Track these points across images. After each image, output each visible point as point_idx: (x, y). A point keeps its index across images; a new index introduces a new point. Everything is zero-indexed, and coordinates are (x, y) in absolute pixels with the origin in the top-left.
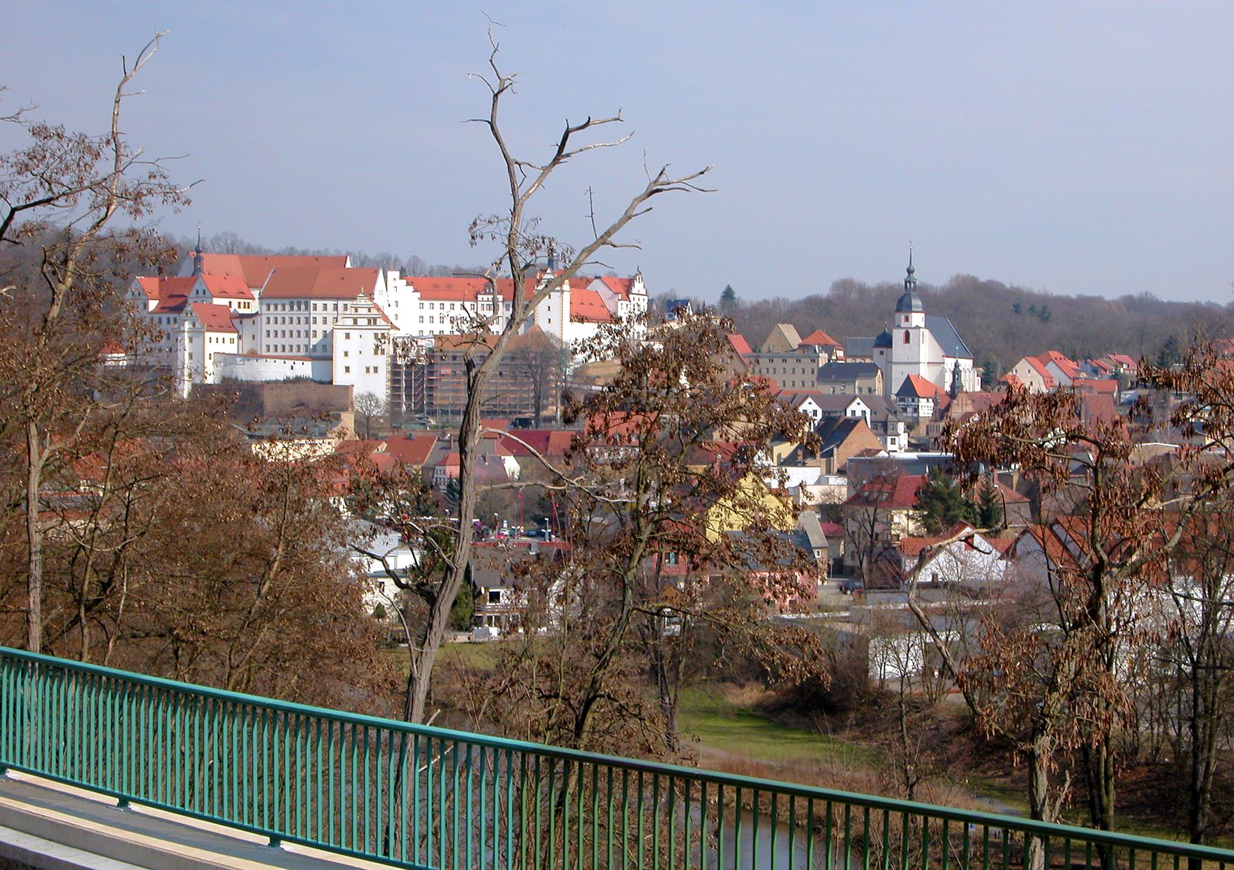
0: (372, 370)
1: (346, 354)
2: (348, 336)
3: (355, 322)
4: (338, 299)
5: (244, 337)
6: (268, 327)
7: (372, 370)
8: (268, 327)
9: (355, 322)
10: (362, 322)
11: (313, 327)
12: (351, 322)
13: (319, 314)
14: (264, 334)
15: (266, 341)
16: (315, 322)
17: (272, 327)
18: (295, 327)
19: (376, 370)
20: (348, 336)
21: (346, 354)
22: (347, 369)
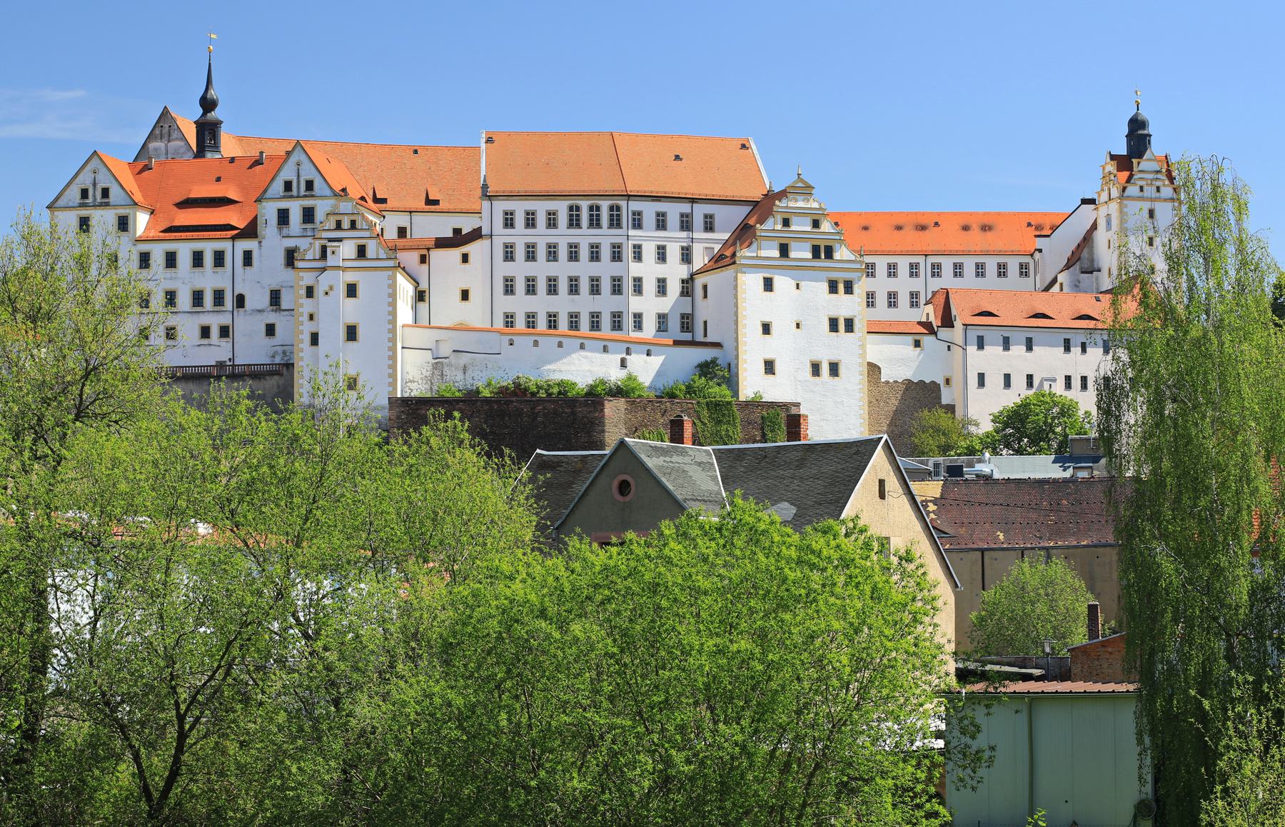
0: (825, 369)
1: (766, 329)
2: (768, 285)
3: (784, 251)
5: (435, 297)
7: (825, 369)
9: (784, 251)
10: (801, 252)
11: (635, 269)
14: (499, 286)
15: (506, 304)
16: (638, 256)
17: (520, 269)
18: (585, 269)
19: (834, 369)
20: (768, 285)
21: (766, 329)
22: (769, 367)
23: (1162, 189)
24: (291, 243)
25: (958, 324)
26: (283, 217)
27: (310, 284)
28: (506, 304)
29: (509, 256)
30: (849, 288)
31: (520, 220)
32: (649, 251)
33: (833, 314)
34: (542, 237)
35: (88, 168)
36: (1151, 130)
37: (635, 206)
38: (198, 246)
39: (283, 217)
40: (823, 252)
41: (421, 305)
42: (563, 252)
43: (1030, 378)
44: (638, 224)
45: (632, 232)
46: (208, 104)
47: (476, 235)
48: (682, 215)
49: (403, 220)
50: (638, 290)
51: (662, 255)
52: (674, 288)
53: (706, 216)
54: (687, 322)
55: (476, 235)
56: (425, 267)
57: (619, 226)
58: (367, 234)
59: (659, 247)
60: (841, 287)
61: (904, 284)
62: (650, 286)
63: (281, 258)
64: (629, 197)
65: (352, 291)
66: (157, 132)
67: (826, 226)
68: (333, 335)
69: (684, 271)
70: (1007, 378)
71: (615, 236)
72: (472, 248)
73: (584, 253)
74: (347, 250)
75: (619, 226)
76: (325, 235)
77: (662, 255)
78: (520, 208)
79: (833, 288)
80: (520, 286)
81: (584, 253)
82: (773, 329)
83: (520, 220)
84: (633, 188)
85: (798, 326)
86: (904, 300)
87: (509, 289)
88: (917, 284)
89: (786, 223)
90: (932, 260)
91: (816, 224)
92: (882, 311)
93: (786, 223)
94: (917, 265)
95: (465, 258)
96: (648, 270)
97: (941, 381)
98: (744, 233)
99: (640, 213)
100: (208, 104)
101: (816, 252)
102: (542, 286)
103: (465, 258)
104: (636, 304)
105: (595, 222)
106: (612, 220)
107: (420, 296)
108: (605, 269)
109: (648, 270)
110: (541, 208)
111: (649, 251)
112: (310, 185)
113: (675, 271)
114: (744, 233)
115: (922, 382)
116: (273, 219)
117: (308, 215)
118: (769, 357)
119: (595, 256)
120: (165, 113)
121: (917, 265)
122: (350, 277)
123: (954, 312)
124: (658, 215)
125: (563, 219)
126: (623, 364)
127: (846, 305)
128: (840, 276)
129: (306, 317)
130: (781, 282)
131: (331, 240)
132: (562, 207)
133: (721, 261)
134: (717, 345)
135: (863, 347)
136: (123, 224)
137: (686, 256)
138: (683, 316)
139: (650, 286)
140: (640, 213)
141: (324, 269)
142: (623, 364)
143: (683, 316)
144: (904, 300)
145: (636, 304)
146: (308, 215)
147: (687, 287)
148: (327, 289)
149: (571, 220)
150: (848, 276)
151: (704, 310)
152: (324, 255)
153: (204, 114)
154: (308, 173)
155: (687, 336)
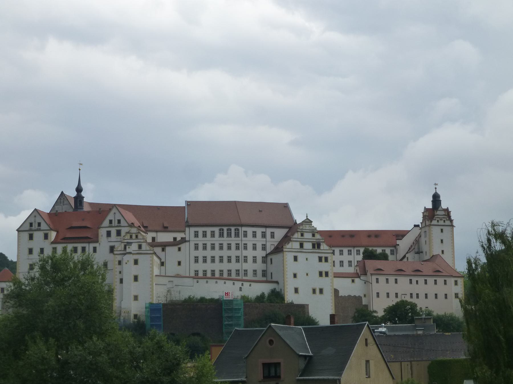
0: (318, 291)
1: (295, 276)
2: (296, 259)
3: (301, 246)
4: (266, 227)
5: (168, 264)
6: (194, 253)
7: (318, 291)
8: (194, 253)
9: (301, 246)
10: (308, 246)
11: (245, 253)
12: (297, 245)
13: (249, 240)
14: (193, 260)
15: (194, 267)
17: (201, 253)
19: (321, 291)
20: (296, 259)
21: (295, 276)
22: (296, 290)
23: (446, 221)
24: (112, 244)
25: (368, 274)
26: (109, 234)
27: (120, 260)
28: (194, 267)
29: (196, 247)
30: (326, 260)
31: (200, 234)
32: (250, 246)
33: (321, 270)
34: (209, 241)
35: (33, 215)
36: (441, 199)
37: (244, 229)
38: (75, 245)
39: (109, 234)
40: (316, 245)
41: (163, 268)
42: (217, 247)
43: (397, 294)
44: (245, 235)
45: (243, 239)
46: (79, 190)
47: (183, 240)
48: (262, 232)
49: (154, 234)
50: (246, 261)
51: (255, 248)
52: (259, 260)
53: (271, 233)
54: (264, 273)
55: (183, 240)
56: (164, 253)
57: (238, 236)
58: (142, 241)
59: (253, 244)
60: (323, 259)
61: (346, 258)
62: (250, 259)
63: (108, 249)
64: (242, 226)
65: (136, 262)
66: (59, 201)
67: (318, 236)
68: (128, 278)
69: (264, 254)
70: (388, 294)
71: (238, 240)
72: (182, 246)
73: (225, 246)
74: (134, 247)
75: (238, 236)
76: (126, 241)
77: (255, 248)
78: (200, 230)
79: (320, 259)
80: (201, 260)
81: (225, 246)
82: (298, 276)
83: (200, 234)
84: (244, 221)
85: (307, 274)
86: (346, 264)
87: (196, 260)
88: (351, 258)
89: (302, 235)
90: (356, 249)
91: (313, 235)
92: (338, 269)
93: (302, 235)
94: (351, 250)
95: (179, 249)
96: (250, 253)
97: (362, 295)
98: (286, 239)
99: (246, 232)
100: (79, 190)
101: (314, 247)
102: (209, 259)
103: (179, 249)
104: (245, 266)
105: (229, 235)
106: (236, 234)
107: (162, 264)
108: (233, 253)
109: (250, 253)
110: (209, 230)
111: (250, 246)
112: (119, 221)
113: (260, 254)
114: (286, 239)
115: (355, 296)
116: (105, 234)
117: (119, 233)
118: (296, 286)
119: (229, 248)
120: (62, 192)
121: (351, 250)
122: (136, 257)
123: (367, 269)
124: (253, 232)
125: (217, 234)
126: (241, 289)
127: (325, 267)
128: (323, 255)
129: (118, 273)
130: (301, 257)
131: (127, 243)
132: (217, 230)
133: (278, 249)
134: (277, 282)
135: (332, 283)
136: (46, 237)
137: (264, 248)
138: (263, 271)
139: (250, 259)
140: (246, 232)
141: (125, 254)
142: (241, 289)
143: (263, 271)
144: (346, 264)
145: (245, 266)
146: (119, 233)
147: (264, 260)
148: (126, 262)
149: (220, 234)
150: (326, 255)
151: (271, 269)
152: (125, 248)
153: (78, 194)
154: (120, 217)
155: (264, 279)
